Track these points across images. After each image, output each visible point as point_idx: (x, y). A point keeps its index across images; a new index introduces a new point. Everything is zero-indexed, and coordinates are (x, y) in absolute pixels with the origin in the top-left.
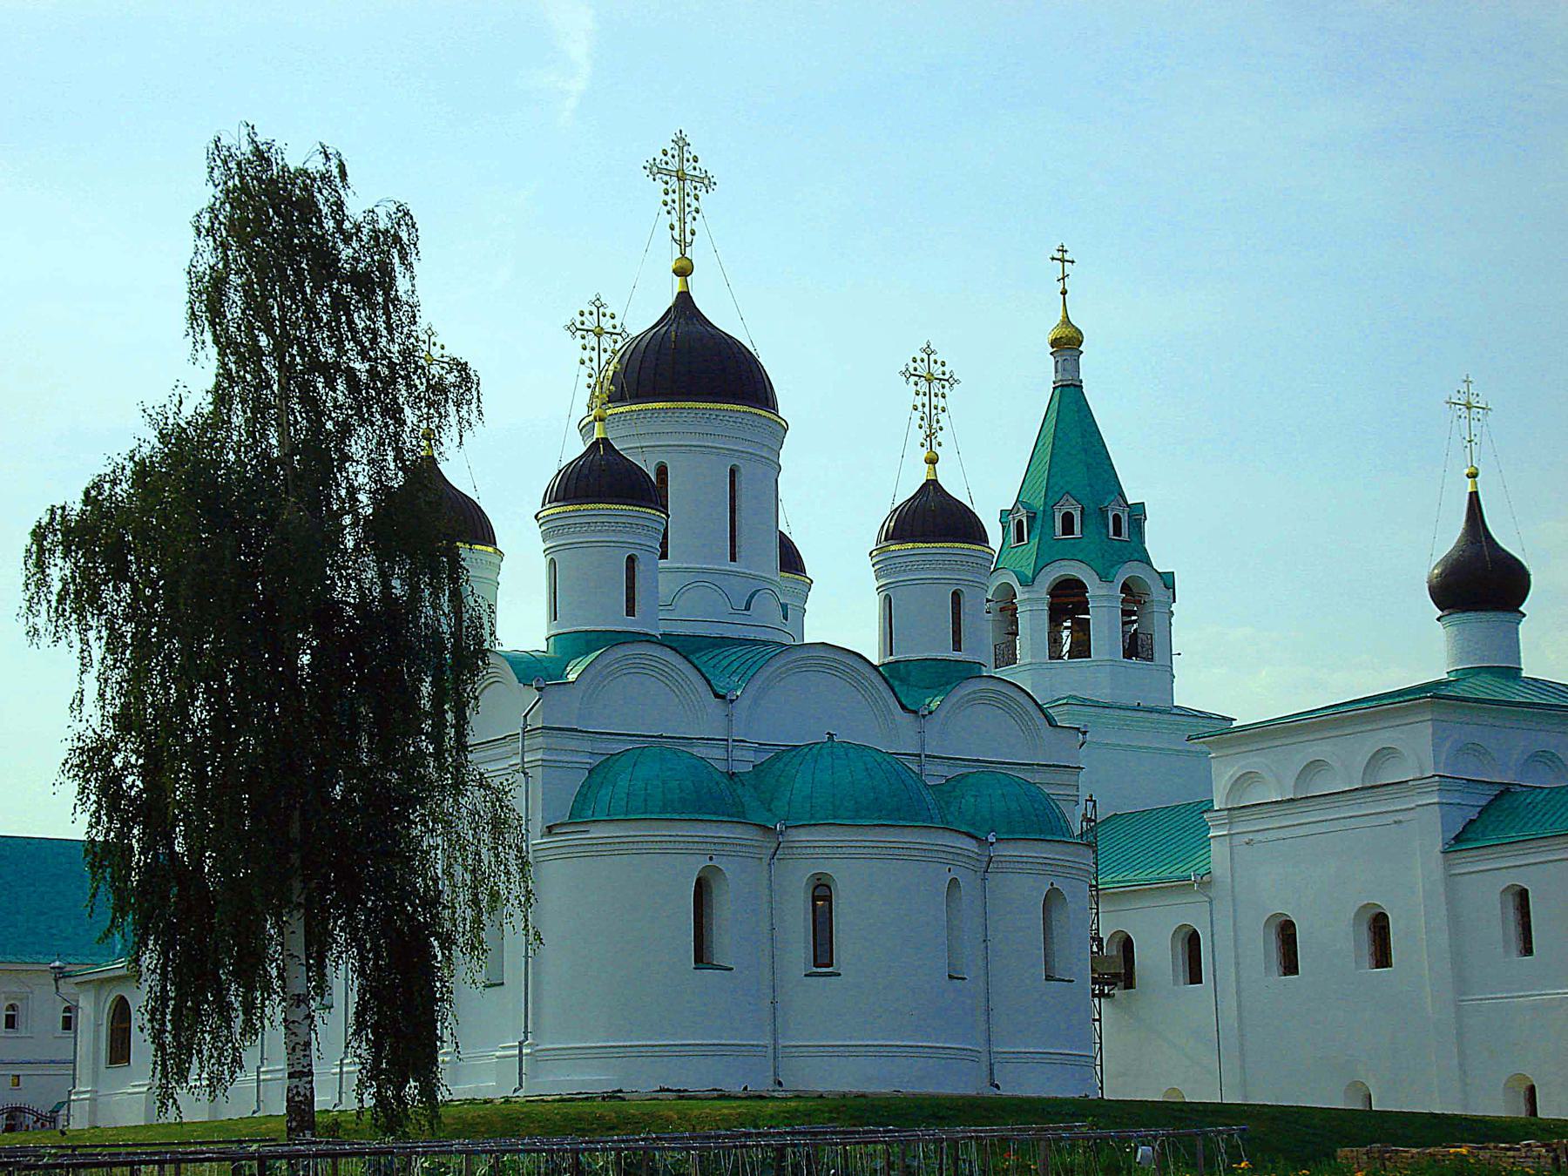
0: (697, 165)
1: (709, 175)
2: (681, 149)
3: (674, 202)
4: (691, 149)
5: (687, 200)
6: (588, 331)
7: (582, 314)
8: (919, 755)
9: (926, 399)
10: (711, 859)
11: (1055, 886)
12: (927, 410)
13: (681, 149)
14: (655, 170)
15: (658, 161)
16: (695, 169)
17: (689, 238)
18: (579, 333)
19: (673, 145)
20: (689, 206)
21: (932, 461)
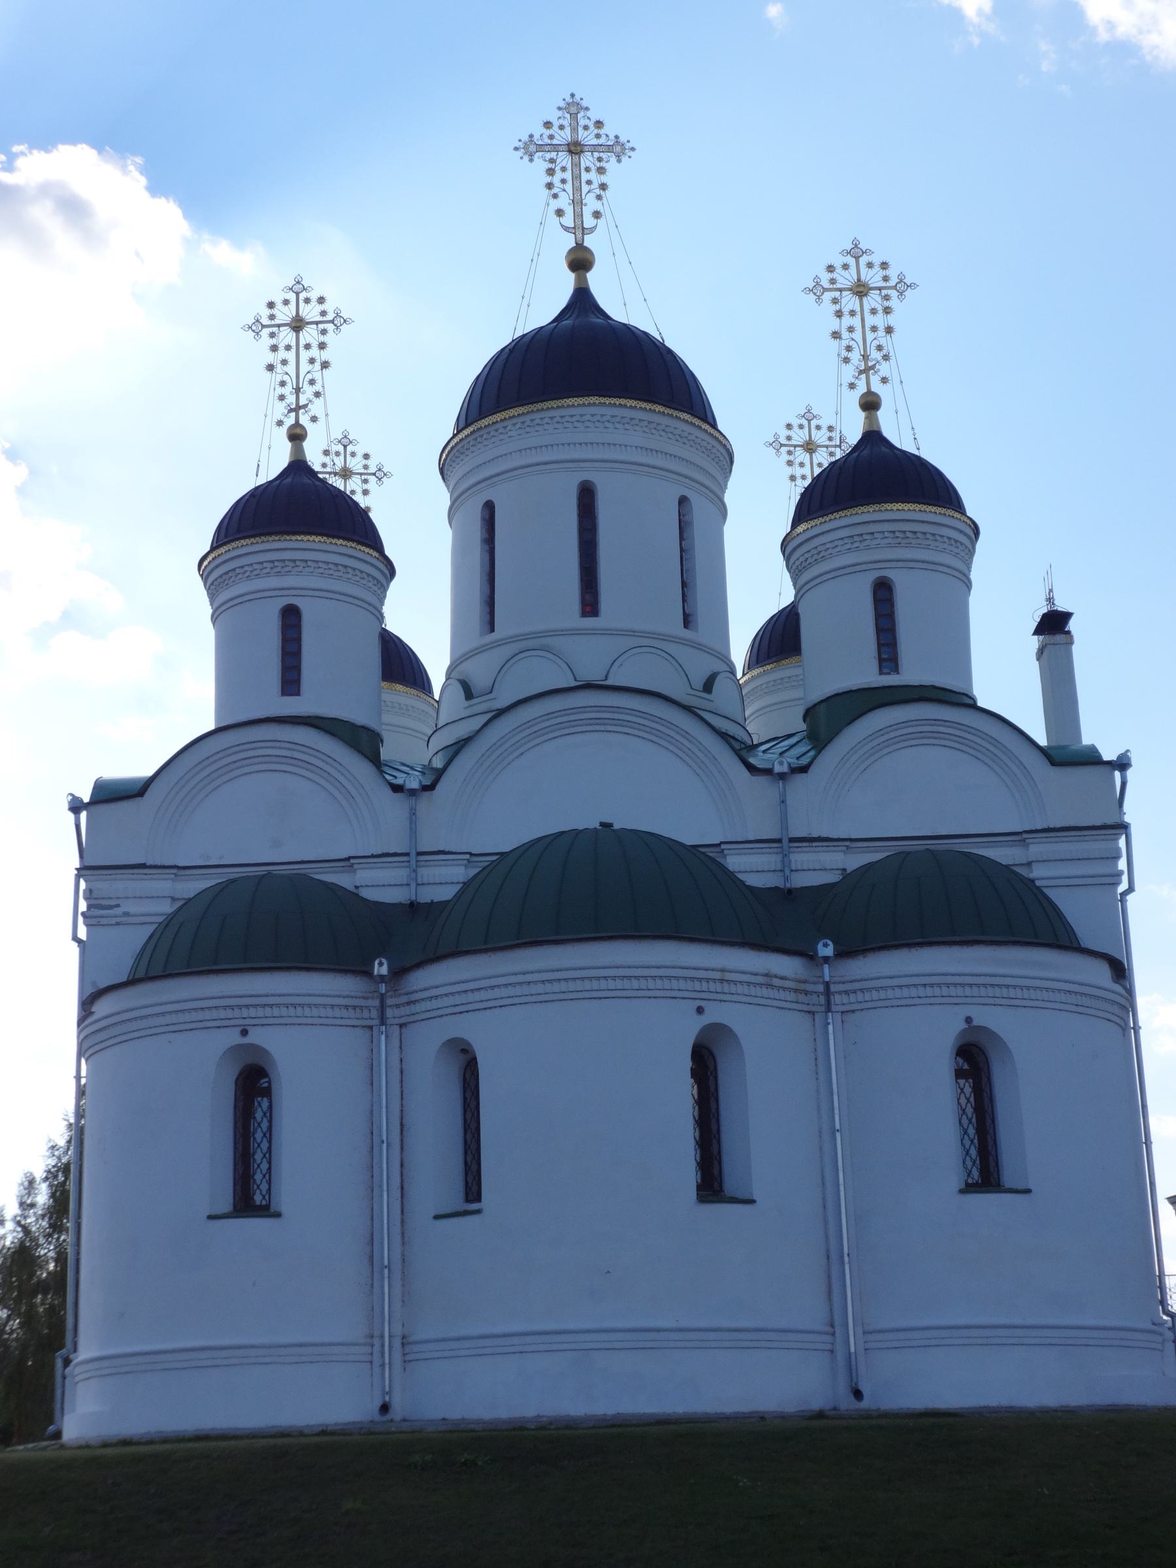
0: (602, 132)
1: (623, 139)
2: (574, 116)
3: (563, 181)
4: (589, 114)
5: (585, 176)
6: (279, 326)
7: (271, 305)
8: (779, 841)
9: (856, 322)
10: (244, 1033)
11: (975, 1023)
12: (858, 335)
13: (574, 116)
14: (532, 148)
15: (536, 137)
16: (598, 136)
17: (589, 222)
18: (266, 331)
19: (560, 113)
20: (589, 182)
21: (870, 404)
